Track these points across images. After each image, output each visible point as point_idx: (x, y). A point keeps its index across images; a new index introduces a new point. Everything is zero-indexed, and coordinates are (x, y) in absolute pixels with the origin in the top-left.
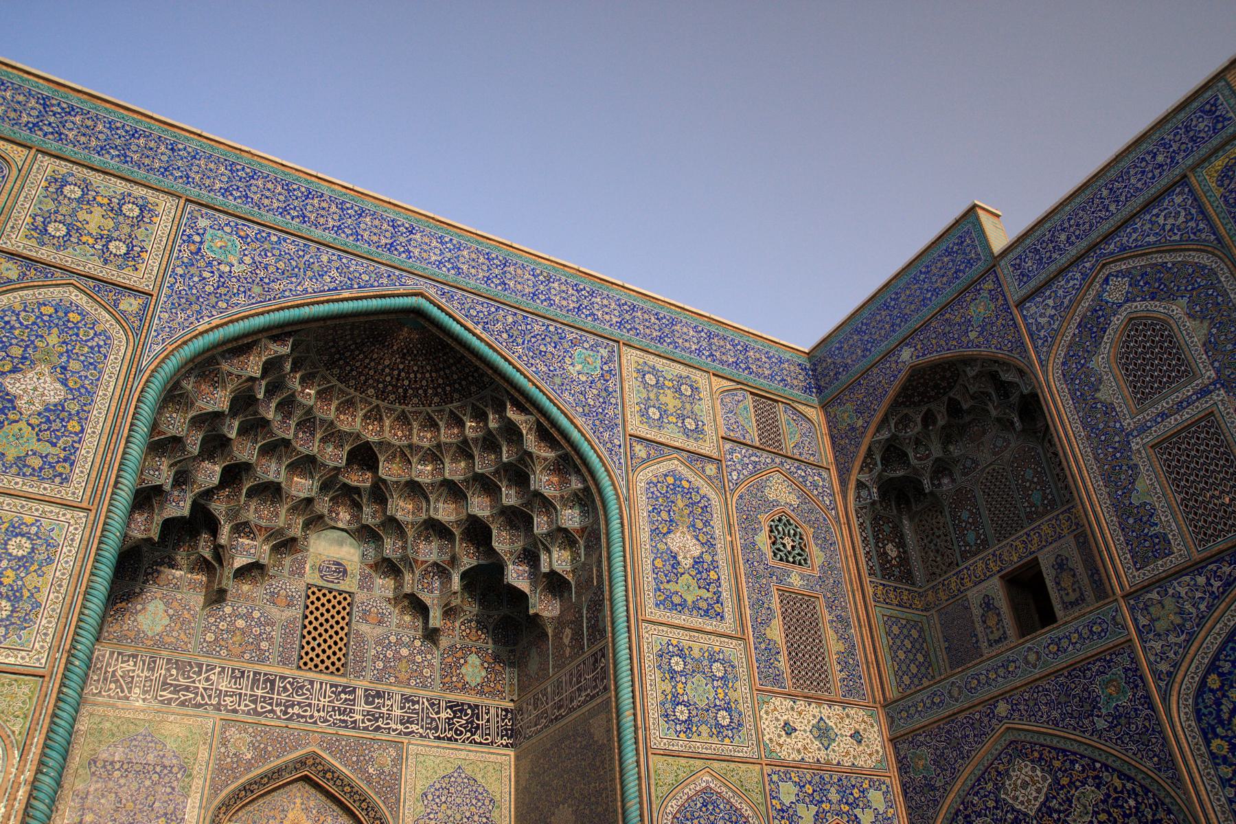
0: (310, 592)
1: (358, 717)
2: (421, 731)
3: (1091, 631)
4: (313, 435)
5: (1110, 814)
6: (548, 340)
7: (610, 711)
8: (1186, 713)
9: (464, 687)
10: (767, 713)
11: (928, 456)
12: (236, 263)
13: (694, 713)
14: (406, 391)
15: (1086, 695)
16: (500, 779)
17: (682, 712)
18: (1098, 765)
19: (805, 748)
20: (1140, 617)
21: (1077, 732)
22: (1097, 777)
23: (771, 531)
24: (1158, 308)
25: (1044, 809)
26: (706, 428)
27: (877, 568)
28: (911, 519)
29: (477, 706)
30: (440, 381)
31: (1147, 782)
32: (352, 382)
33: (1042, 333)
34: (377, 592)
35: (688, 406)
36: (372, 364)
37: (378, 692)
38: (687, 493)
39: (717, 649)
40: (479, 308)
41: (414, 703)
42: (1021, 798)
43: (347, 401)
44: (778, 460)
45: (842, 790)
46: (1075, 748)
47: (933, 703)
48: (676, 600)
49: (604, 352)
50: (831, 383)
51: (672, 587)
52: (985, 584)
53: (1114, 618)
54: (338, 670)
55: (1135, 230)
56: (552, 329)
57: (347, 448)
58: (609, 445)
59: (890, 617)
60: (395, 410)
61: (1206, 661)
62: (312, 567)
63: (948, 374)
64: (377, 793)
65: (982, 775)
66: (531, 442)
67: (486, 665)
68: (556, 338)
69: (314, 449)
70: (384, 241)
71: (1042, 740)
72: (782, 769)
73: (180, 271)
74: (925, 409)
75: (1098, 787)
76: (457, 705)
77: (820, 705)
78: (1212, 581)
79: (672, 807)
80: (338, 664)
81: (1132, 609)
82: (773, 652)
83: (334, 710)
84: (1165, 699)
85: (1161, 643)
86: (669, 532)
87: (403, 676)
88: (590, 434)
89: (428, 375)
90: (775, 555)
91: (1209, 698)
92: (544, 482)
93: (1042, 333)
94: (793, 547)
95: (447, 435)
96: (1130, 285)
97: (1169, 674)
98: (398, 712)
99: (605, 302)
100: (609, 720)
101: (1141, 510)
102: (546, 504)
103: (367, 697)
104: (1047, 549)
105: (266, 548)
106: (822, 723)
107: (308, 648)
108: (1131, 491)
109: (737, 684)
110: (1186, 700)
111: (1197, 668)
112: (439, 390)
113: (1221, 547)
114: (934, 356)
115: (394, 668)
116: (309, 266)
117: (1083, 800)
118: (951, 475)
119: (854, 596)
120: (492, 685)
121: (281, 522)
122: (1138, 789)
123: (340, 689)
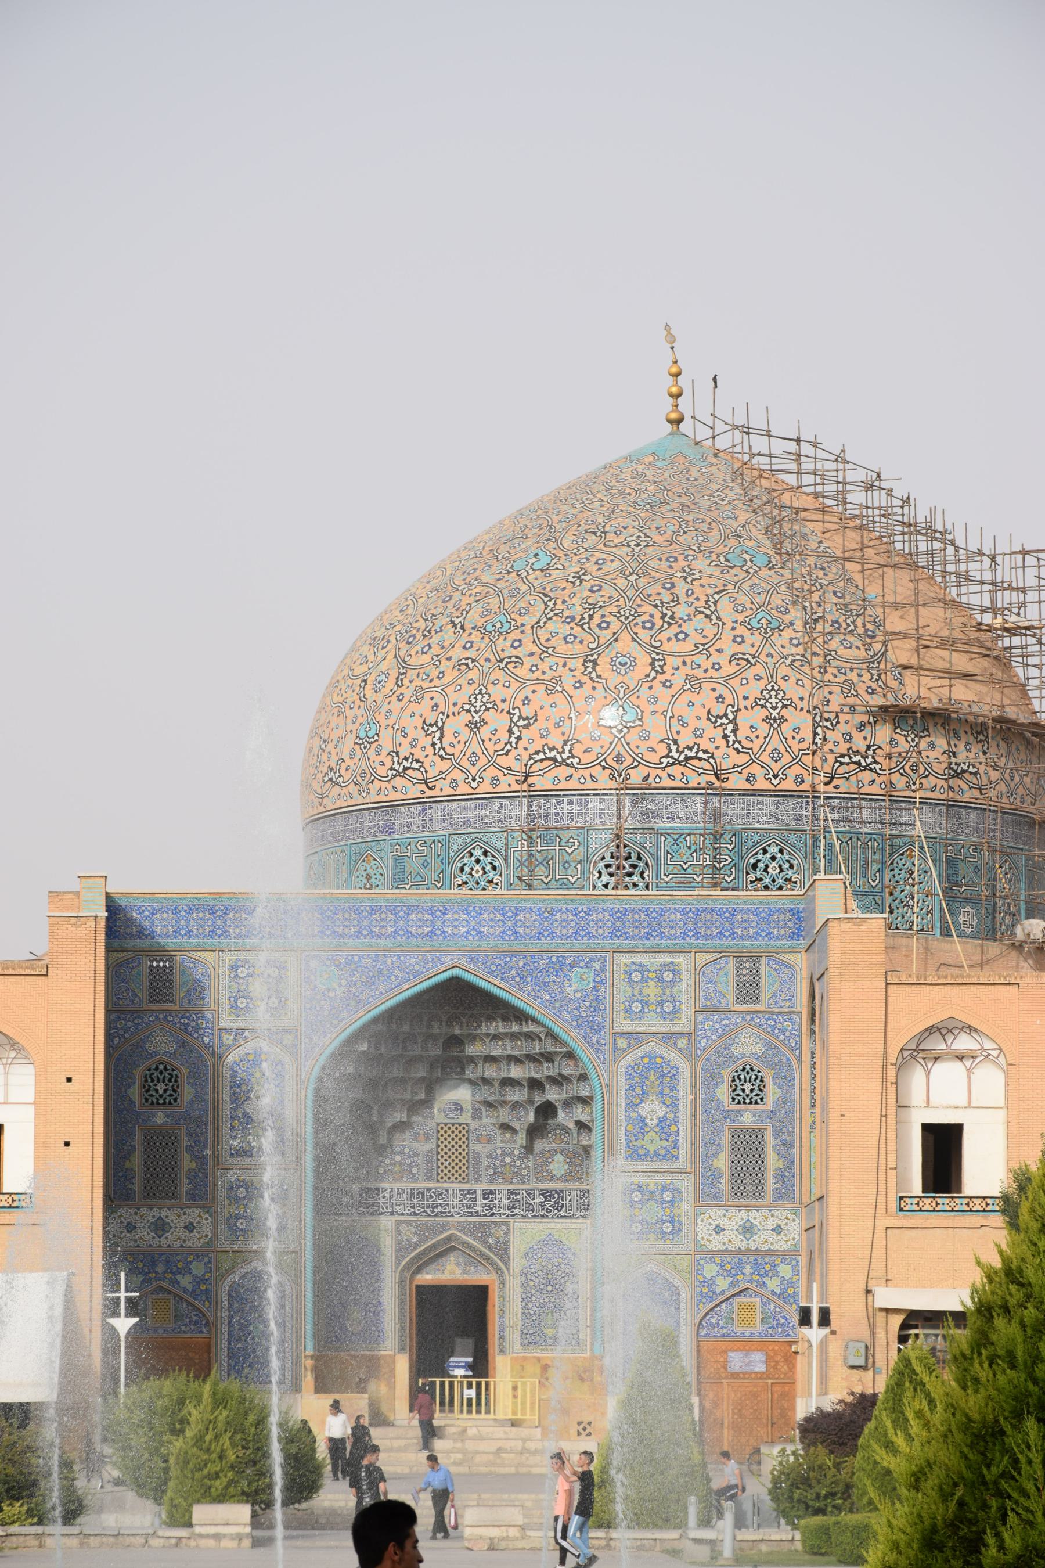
1: (479, 1209)
10: (702, 1221)
12: (337, 987)
23: (734, 1081)
26: (682, 1007)
29: (562, 1191)
34: (484, 1121)
35: (668, 991)
39: (668, 1182)
40: (497, 962)
41: (517, 1194)
44: (748, 1017)
48: (641, 1152)
49: (597, 965)
51: (639, 1143)
56: (554, 959)
58: (596, 1046)
62: (439, 1110)
68: (557, 967)
70: (426, 930)
73: (308, 1006)
80: (464, 1175)
87: (509, 1176)
90: (734, 1099)
94: (752, 1091)
98: (505, 1202)
99: (600, 916)
103: (484, 1195)
107: (442, 1167)
109: (682, 1205)
116: (380, 973)
119: (801, 1123)
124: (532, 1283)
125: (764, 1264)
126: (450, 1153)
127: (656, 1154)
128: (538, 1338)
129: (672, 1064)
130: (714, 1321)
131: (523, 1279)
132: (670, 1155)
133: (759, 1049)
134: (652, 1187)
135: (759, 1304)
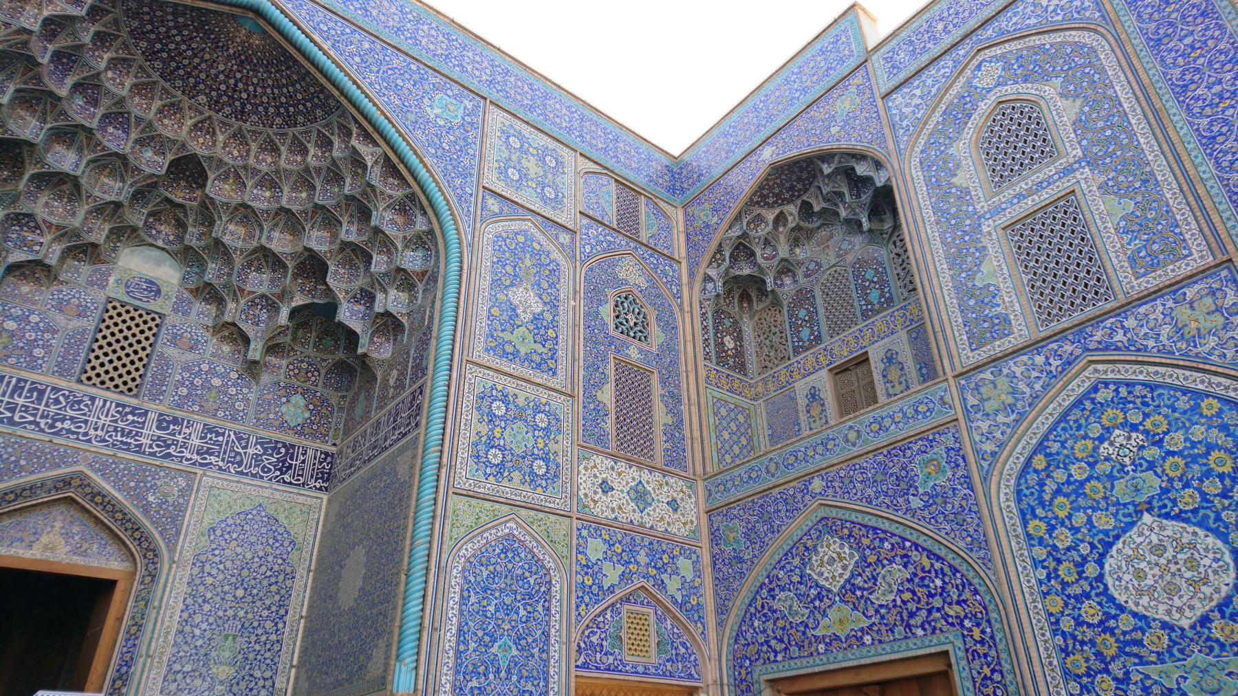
0: (110, 306)
1: (144, 441)
2: (221, 464)
3: (916, 411)
4: (126, 131)
5: (914, 593)
6: (407, 76)
7: (417, 448)
8: (1006, 494)
9: (281, 426)
10: (586, 468)
11: (774, 256)
13: (509, 458)
14: (243, 105)
15: (903, 473)
16: (306, 522)
17: (495, 456)
18: (908, 544)
19: (620, 508)
20: (969, 397)
21: (891, 511)
22: (906, 556)
24: (1029, 90)
25: (848, 587)
27: (713, 354)
28: (752, 317)
29: (293, 446)
30: (283, 100)
31: (956, 563)
32: (179, 83)
33: (904, 124)
36: (204, 66)
37: (175, 418)
38: (536, 254)
39: (544, 401)
41: (218, 434)
42: (826, 575)
43: (173, 105)
45: (652, 553)
46: (886, 525)
47: (750, 477)
48: (509, 349)
50: (693, 184)
51: (506, 336)
52: (812, 377)
53: (942, 398)
54: (130, 390)
55: (1015, 14)
57: (170, 157)
58: (459, 191)
59: (719, 399)
60: (231, 126)
61: (1034, 441)
62: (117, 281)
63: (805, 175)
64: (153, 523)
65: (790, 551)
66: (375, 175)
67: (311, 407)
69: (127, 148)
71: (853, 518)
72: (593, 525)
74: (777, 211)
75: (905, 566)
76: (270, 442)
77: (641, 469)
78: (1051, 361)
79: (468, 550)
81: (962, 389)
82: (601, 413)
83: (116, 430)
84: (985, 480)
85: (989, 423)
86: (512, 285)
87: (210, 405)
88: (439, 177)
89: (269, 91)
91: (1032, 478)
92: (383, 217)
93: (904, 124)
94: (635, 324)
95: (287, 160)
96: (1004, 69)
97: (993, 454)
98: (197, 442)
100: (414, 457)
101: (985, 292)
102: (387, 245)
103: (160, 422)
104: (876, 345)
105: (58, 248)
106: (640, 487)
108: (975, 274)
109: (560, 437)
110: (1008, 480)
111: (1024, 448)
112: (282, 110)
113: (1066, 325)
114: (795, 152)
115: (202, 396)
117: (888, 579)
118: (794, 275)
120: (315, 427)
121: (77, 222)
122: (946, 569)
123: (128, 410)
124: (209, 580)
125: (663, 553)
126: (116, 346)
127: (528, 358)
128: (198, 682)
129: (552, 256)
130: (594, 639)
131: (195, 571)
132: (546, 364)
133: (642, 282)
134: (521, 401)
135: (652, 618)
